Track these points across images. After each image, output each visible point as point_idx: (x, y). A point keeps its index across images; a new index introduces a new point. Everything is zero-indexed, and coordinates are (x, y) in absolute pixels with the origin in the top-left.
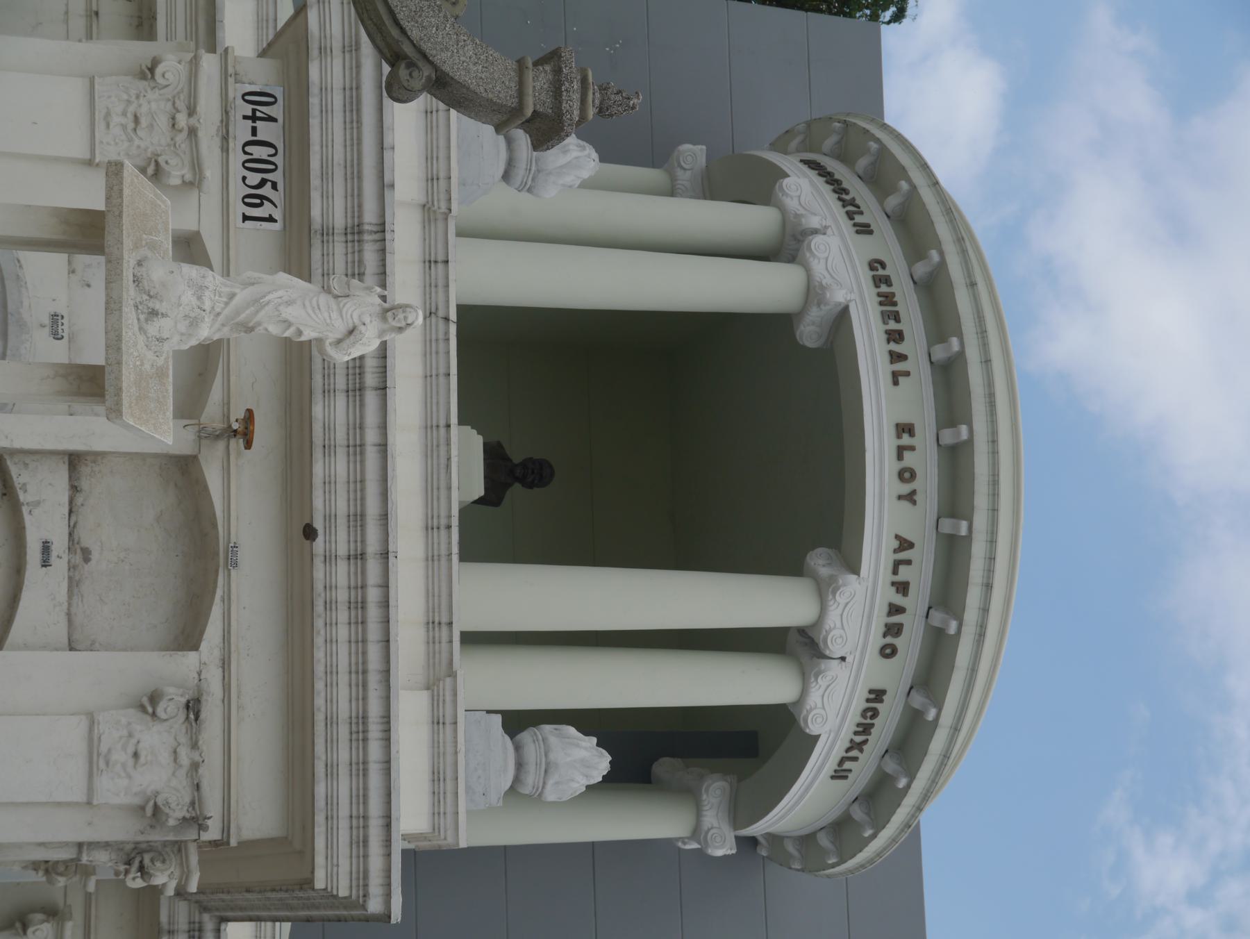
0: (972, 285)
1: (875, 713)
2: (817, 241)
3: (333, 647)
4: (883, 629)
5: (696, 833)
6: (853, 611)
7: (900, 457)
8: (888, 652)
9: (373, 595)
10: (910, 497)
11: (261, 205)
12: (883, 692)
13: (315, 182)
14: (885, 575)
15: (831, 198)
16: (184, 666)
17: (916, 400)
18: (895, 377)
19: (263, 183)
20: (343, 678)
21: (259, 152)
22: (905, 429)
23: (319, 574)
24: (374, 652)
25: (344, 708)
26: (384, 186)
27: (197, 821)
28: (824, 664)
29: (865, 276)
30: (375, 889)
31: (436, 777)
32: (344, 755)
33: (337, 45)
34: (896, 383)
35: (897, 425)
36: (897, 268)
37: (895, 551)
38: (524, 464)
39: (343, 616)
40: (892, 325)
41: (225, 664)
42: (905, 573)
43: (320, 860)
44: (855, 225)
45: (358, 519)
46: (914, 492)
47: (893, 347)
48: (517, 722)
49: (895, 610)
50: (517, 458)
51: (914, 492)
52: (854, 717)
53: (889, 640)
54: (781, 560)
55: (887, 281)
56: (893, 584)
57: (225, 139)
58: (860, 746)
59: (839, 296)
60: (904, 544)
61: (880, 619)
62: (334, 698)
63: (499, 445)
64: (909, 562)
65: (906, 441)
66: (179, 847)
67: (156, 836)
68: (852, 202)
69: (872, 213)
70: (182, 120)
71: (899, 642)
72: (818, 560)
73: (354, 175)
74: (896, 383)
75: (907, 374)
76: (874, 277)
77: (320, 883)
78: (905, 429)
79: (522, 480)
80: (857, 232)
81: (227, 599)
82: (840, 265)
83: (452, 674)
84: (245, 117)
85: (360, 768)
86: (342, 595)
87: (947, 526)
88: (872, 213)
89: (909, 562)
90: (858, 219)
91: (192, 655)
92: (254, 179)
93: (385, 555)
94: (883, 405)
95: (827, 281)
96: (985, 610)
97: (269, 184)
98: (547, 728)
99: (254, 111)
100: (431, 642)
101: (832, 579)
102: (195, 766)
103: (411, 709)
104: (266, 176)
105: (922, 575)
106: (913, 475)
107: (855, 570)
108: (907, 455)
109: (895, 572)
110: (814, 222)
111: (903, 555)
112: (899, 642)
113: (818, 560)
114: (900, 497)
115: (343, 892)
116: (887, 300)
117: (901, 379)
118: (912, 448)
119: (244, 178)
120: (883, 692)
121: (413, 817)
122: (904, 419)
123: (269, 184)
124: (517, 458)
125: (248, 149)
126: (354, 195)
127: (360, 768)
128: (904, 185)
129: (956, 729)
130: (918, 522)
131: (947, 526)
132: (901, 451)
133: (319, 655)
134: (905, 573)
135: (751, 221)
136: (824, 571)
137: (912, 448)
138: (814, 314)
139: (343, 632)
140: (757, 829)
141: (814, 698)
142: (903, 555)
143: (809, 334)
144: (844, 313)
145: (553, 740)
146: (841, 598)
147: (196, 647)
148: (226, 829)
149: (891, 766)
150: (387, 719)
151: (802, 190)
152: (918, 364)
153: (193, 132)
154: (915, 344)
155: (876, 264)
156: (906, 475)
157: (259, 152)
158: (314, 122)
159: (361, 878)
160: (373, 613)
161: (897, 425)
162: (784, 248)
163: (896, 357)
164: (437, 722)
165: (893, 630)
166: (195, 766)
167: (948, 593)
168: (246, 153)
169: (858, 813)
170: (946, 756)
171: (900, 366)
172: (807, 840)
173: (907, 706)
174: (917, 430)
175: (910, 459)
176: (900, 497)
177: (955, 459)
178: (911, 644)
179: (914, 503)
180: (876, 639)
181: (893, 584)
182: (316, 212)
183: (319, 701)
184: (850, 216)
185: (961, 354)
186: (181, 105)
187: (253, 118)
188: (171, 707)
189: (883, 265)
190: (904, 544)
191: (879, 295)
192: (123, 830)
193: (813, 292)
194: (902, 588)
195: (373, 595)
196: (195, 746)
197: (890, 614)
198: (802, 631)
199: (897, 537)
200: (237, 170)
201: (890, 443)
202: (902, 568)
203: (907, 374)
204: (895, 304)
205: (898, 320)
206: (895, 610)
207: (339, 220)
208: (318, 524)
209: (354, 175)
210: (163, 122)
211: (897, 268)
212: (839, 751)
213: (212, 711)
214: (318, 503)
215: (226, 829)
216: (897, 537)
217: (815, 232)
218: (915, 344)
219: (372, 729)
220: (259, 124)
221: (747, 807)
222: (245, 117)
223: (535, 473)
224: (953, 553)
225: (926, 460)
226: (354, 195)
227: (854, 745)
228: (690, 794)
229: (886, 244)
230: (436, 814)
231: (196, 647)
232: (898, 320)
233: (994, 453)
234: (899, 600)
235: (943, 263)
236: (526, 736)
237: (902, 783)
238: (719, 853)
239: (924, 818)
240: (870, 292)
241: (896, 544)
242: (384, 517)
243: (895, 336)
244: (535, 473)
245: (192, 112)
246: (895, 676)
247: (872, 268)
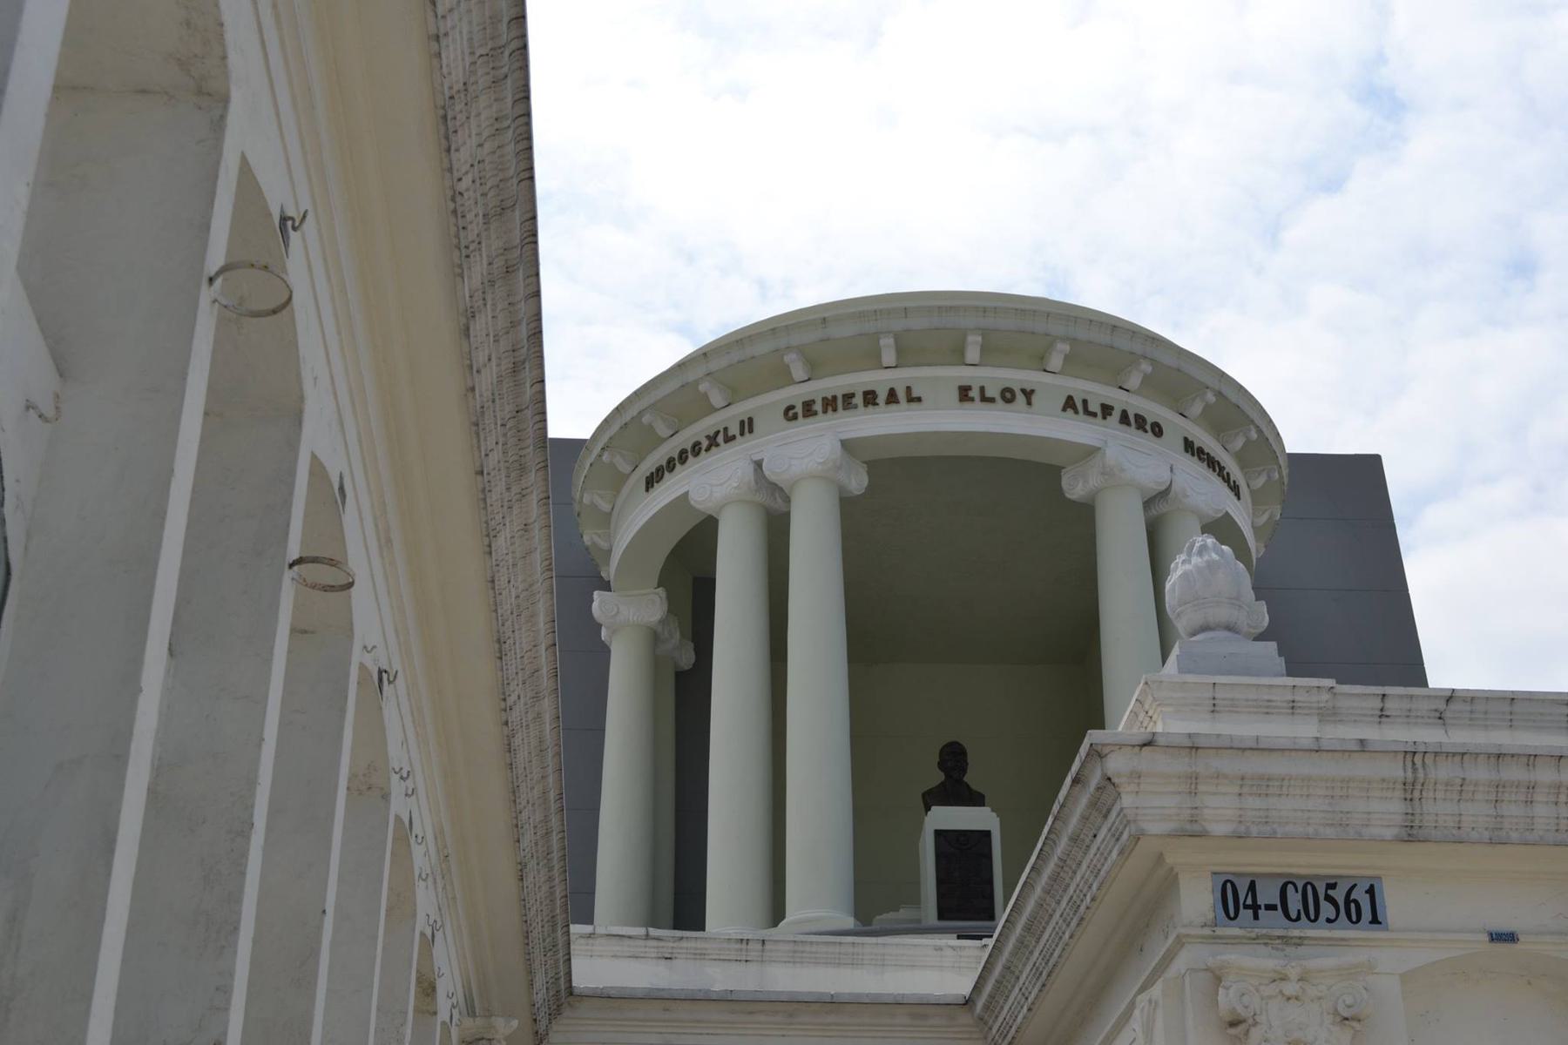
4: (1140, 432)
7: (992, 400)
8: (1157, 430)
10: (1028, 394)
11: (1355, 901)
12: (1186, 439)
19: (1329, 899)
21: (1295, 903)
22: (964, 393)
34: (919, 399)
35: (961, 400)
37: (1076, 412)
42: (1094, 407)
44: (742, 434)
46: (1023, 391)
51: (1023, 391)
53: (1148, 427)
56: (1104, 418)
58: (1222, 469)
60: (1070, 404)
64: (1085, 402)
65: (975, 393)
71: (1150, 420)
74: (919, 399)
75: (909, 388)
76: (805, 416)
80: (751, 431)
84: (1256, 917)
89: (1085, 402)
90: (734, 430)
92: (1327, 910)
97: (1330, 892)
99: (1246, 907)
104: (1322, 897)
108: (989, 394)
109: (1094, 415)
113: (1075, 487)
114: (1029, 403)
116: (830, 404)
117: (914, 395)
118: (982, 389)
119: (1329, 921)
120: (1186, 439)
122: (955, 394)
123: (1330, 892)
124: (938, 777)
125: (1294, 915)
132: (985, 399)
137: (982, 389)
143: (857, 482)
154: (878, 380)
155: (789, 414)
156: (1008, 396)
157: (1295, 903)
161: (961, 400)
163: (892, 397)
165: (1140, 422)
168: (1298, 918)
171: (901, 394)
174: (965, 383)
176: (1029, 403)
179: (1032, 391)
181: (1104, 418)
184: (729, 439)
187: (1255, 908)
189: (791, 407)
190: (1070, 404)
191: (825, 412)
197: (1128, 424)
198: (1147, 504)
199: (1064, 409)
202: (1091, 409)
203: (909, 388)
204: (835, 398)
205: (852, 395)
206: (1124, 419)
211: (795, 394)
216: (1064, 409)
220: (1261, 901)
222: (1256, 917)
223: (953, 757)
227: (1221, 474)
232: (852, 395)
234: (1116, 414)
241: (1070, 412)
243: (870, 398)
247: (795, 417)
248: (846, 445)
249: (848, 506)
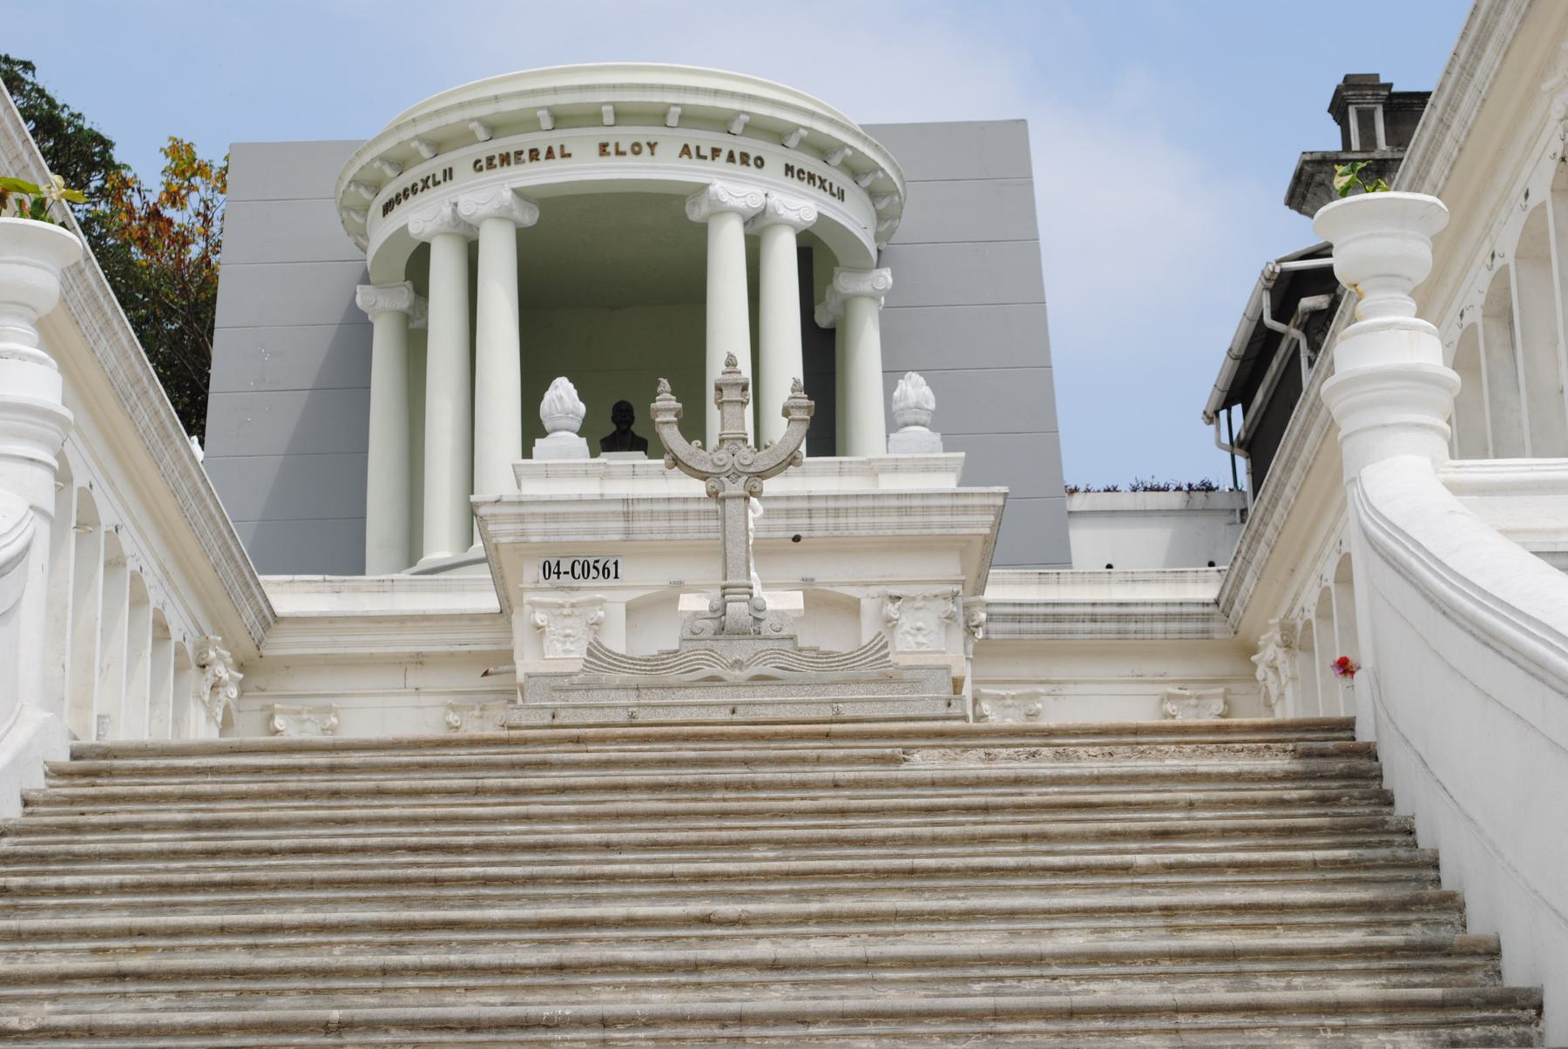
0: (496, 98)
1: (801, 171)
2: (464, 211)
3: (860, 525)
5: (874, 297)
6: (735, 190)
7: (624, 154)
8: (760, 162)
9: (832, 504)
10: (652, 146)
13: (599, 538)
14: (708, 165)
15: (420, 198)
16: (868, 606)
17: (582, 141)
18: (565, 155)
20: (877, 520)
21: (578, 570)
22: (603, 149)
23: (819, 533)
24: (862, 503)
25: (894, 519)
26: (602, 500)
27: (955, 595)
28: (770, 210)
29: (487, 175)
30: (991, 501)
31: (926, 469)
32: (919, 519)
33: (520, 527)
39: (842, 520)
41: (867, 584)
42: (706, 151)
43: (975, 531)
45: (789, 513)
47: (542, 155)
48: (893, 424)
49: (731, 158)
50: (613, 428)
52: (804, 186)
53: (751, 162)
55: (490, 160)
57: (572, 589)
58: (823, 181)
59: (507, 195)
61: (737, 168)
62: (888, 524)
63: (603, 441)
65: (611, 149)
66: (966, 607)
67: (961, 620)
68: (425, 182)
69: (436, 166)
70: (566, 611)
71: (752, 156)
73: (595, 516)
77: (987, 531)
81: (832, 584)
83: (869, 462)
85: (926, 510)
86: (831, 521)
90: (440, 177)
91: (863, 602)
92: (593, 572)
93: (810, 498)
94: (584, 168)
96: (733, 95)
98: (894, 408)
100: (850, 473)
102: (925, 598)
103: (890, 484)
105: (706, 139)
106: (637, 144)
107: (705, 187)
110: (447, 211)
112: (752, 156)
113: (695, 214)
115: (992, 518)
116: (505, 159)
117: (567, 151)
118: (617, 145)
121: (947, 482)
122: (596, 150)
124: (613, 428)
126: (607, 516)
127: (926, 510)
128: (414, 144)
129: (813, 115)
131: (673, 121)
132: (618, 153)
133: (864, 533)
134: (706, 151)
137: (617, 145)
138: (517, 214)
139: (852, 520)
140: (872, 249)
141: (793, 216)
143: (529, 218)
145: (901, 405)
146: (725, 198)
147: (858, 602)
148: (956, 582)
149: (836, 160)
150: (899, 496)
151: (422, 217)
152: (555, 138)
153: (573, 606)
154: (541, 141)
156: (636, 149)
157: (578, 570)
158: (565, 539)
159: (984, 509)
160: (841, 504)
163: (550, 154)
164: (896, 469)
165: (745, 158)
166: (925, 598)
167: (721, 122)
169: (866, 182)
170: (831, 121)
171: (557, 152)
172: (881, 217)
173: (796, 149)
174: (604, 141)
177: (623, 115)
178: (754, 147)
180: (752, 171)
182: (617, 537)
183: (889, 532)
184: (436, 184)
185: (549, 108)
186: (558, 612)
188: (891, 609)
189: (478, 161)
190: (686, 150)
192: (958, 634)
193: (502, 217)
194: (716, 152)
195: (832, 504)
196: (914, 599)
198: (745, 224)
200: (589, 583)
202: (702, 153)
205: (521, 153)
207: (621, 525)
208: (793, 534)
209: (595, 516)
210: (569, 621)
211: (482, 151)
212: (826, 197)
213: (896, 591)
214: (781, 534)
215: (956, 582)
219: (905, 504)
221: (862, 266)
224: (691, 118)
225: (625, 135)
226: (607, 516)
228: (846, 303)
229: (461, 159)
230: (946, 470)
231: (858, 602)
232: (521, 153)
233: (623, 87)
234: (724, 155)
235: (480, 120)
236: (900, 421)
237: (849, 152)
238: (890, 280)
239: (855, 121)
240: (500, 172)
242: (789, 498)
243: (534, 155)
245: (562, 606)
246: (776, 158)
247: (481, 169)
248: (515, 191)
249: (524, 239)
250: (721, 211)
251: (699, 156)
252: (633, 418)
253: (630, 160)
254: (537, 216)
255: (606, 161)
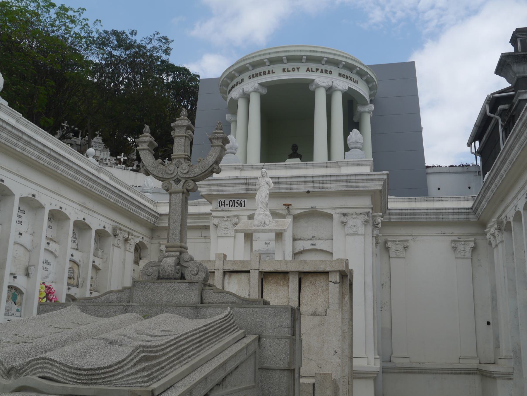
0: (253, 57)
1: (344, 75)
2: (245, 90)
3: (332, 187)
5: (369, 112)
6: (322, 80)
7: (290, 71)
8: (331, 72)
9: (321, 179)
10: (298, 69)
13: (237, 192)
14: (314, 74)
15: (236, 88)
16: (336, 217)
17: (278, 68)
18: (273, 73)
20: (338, 184)
22: (284, 70)
23: (317, 190)
24: (333, 178)
25: (345, 184)
26: (237, 178)
27: (368, 213)
28: (333, 86)
29: (252, 80)
30: (382, 177)
31: (358, 165)
32: (354, 184)
33: (209, 189)
36: (250, 73)
38: (293, 150)
39: (325, 185)
40: (262, 74)
41: (335, 209)
42: (314, 70)
43: (376, 188)
45: (305, 182)
47: (267, 73)
48: (347, 149)
49: (322, 71)
52: (344, 79)
54: (312, 95)
55: (253, 75)
57: (229, 211)
58: (351, 78)
59: (256, 85)
60: (308, 70)
61: (324, 74)
62: (342, 186)
65: (286, 70)
66: (373, 217)
67: (371, 222)
68: (237, 83)
69: (239, 79)
70: (225, 219)
71: (329, 70)
72: (312, 88)
73: (235, 185)
77: (381, 188)
78: (284, 70)
79: (296, 150)
81: (322, 208)
82: (250, 85)
83: (337, 162)
85: (357, 181)
86: (321, 185)
87: (304, 61)
88: (239, 79)
91: (334, 215)
92: (236, 205)
93: (313, 177)
94: (279, 75)
95: (253, 88)
96: (322, 52)
98: (348, 142)
100: (330, 167)
101: (315, 85)
102: (357, 214)
103: (345, 170)
105: (314, 66)
107: (314, 80)
110: (241, 91)
111: (310, 70)
112: (329, 70)
113: (312, 88)
115: (382, 183)
116: (257, 75)
121: (367, 170)
124: (291, 152)
126: (239, 184)
127: (357, 181)
128: (233, 72)
129: (347, 58)
130: (303, 67)
131: (304, 61)
132: (289, 71)
133: (333, 190)
134: (314, 70)
135: (241, 104)
136: (314, 87)
138: (260, 90)
139: (329, 185)
140: (368, 100)
141: (341, 88)
142: (310, 70)
143: (264, 91)
144: (260, 84)
145: (351, 141)
146: (320, 83)
147: (332, 215)
148: (369, 208)
149: (355, 71)
150: (347, 175)
151: (235, 94)
152: (270, 68)
153: (228, 217)
156: (293, 70)
158: (225, 193)
159: (379, 180)
160: (325, 179)
162: (247, 97)
163: (269, 73)
164: (347, 165)
165: (326, 71)
166: (357, 214)
167: (317, 60)
169: (365, 78)
170: (352, 60)
172: (371, 89)
173: (342, 68)
175: (290, 69)
177: (290, 59)
178: (329, 68)
180: (328, 75)
182: (243, 192)
183: (343, 189)
184: (240, 83)
185: (268, 59)
186: (222, 219)
187: (224, 205)
188: (344, 219)
190: (308, 70)
192: (370, 228)
193: (256, 91)
194: (317, 70)
195: (321, 179)
196: (352, 214)
198: (327, 91)
200: (235, 208)
201: (287, 73)
207: (244, 187)
208: (307, 190)
209: (235, 185)
210: (226, 223)
211: (250, 73)
212: (352, 83)
213: (345, 211)
214: (302, 190)
215: (369, 208)
217: (243, 91)
218: (266, 69)
219: (348, 178)
221: (364, 103)
223: (295, 148)
224: (310, 59)
225: (290, 66)
226: (239, 184)
227: (350, 79)
228: (361, 114)
230: (366, 165)
231: (332, 215)
233: (288, 51)
234: (320, 71)
235: (249, 63)
236: (350, 147)
237: (358, 69)
238: (373, 107)
239: (366, 64)
240: (256, 79)
242: (305, 177)
243: (265, 73)
244: (295, 148)
245: (224, 217)
246: (336, 71)
248: (259, 84)
250: (318, 86)
251: (312, 71)
252: (297, 149)
253: (292, 73)
254: (267, 91)
255: (285, 74)
